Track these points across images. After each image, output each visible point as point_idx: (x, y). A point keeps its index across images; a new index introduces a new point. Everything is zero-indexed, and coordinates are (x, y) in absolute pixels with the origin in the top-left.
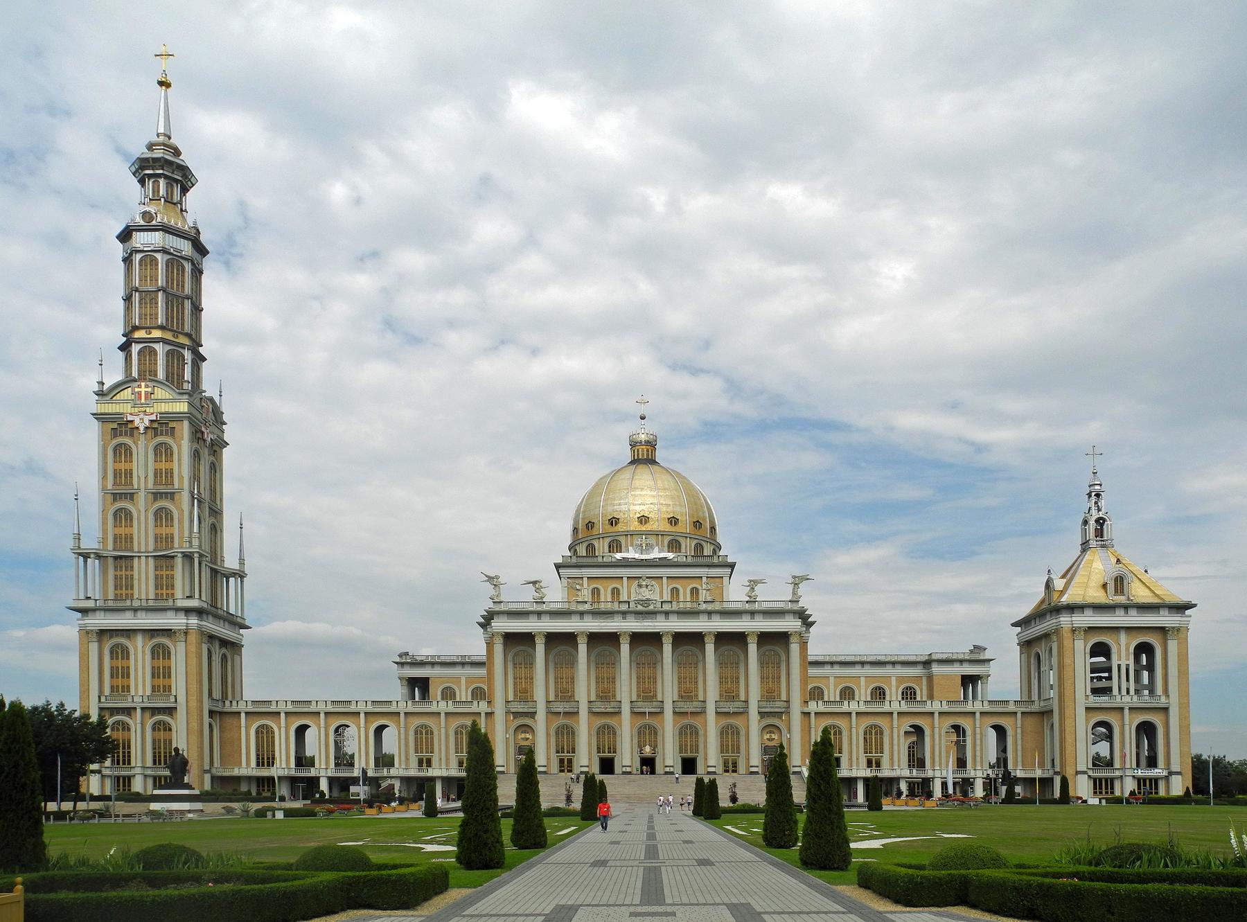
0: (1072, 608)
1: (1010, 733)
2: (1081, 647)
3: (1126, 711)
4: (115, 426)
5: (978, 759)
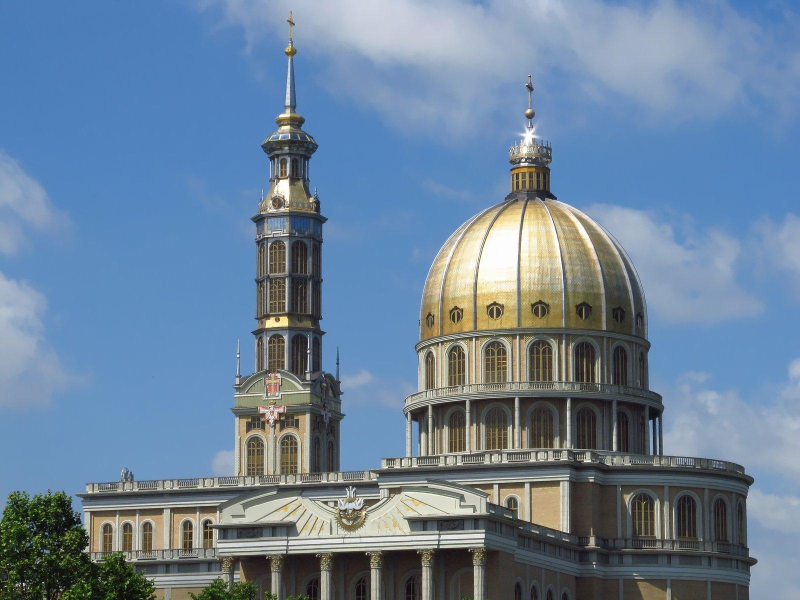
4: (250, 420)
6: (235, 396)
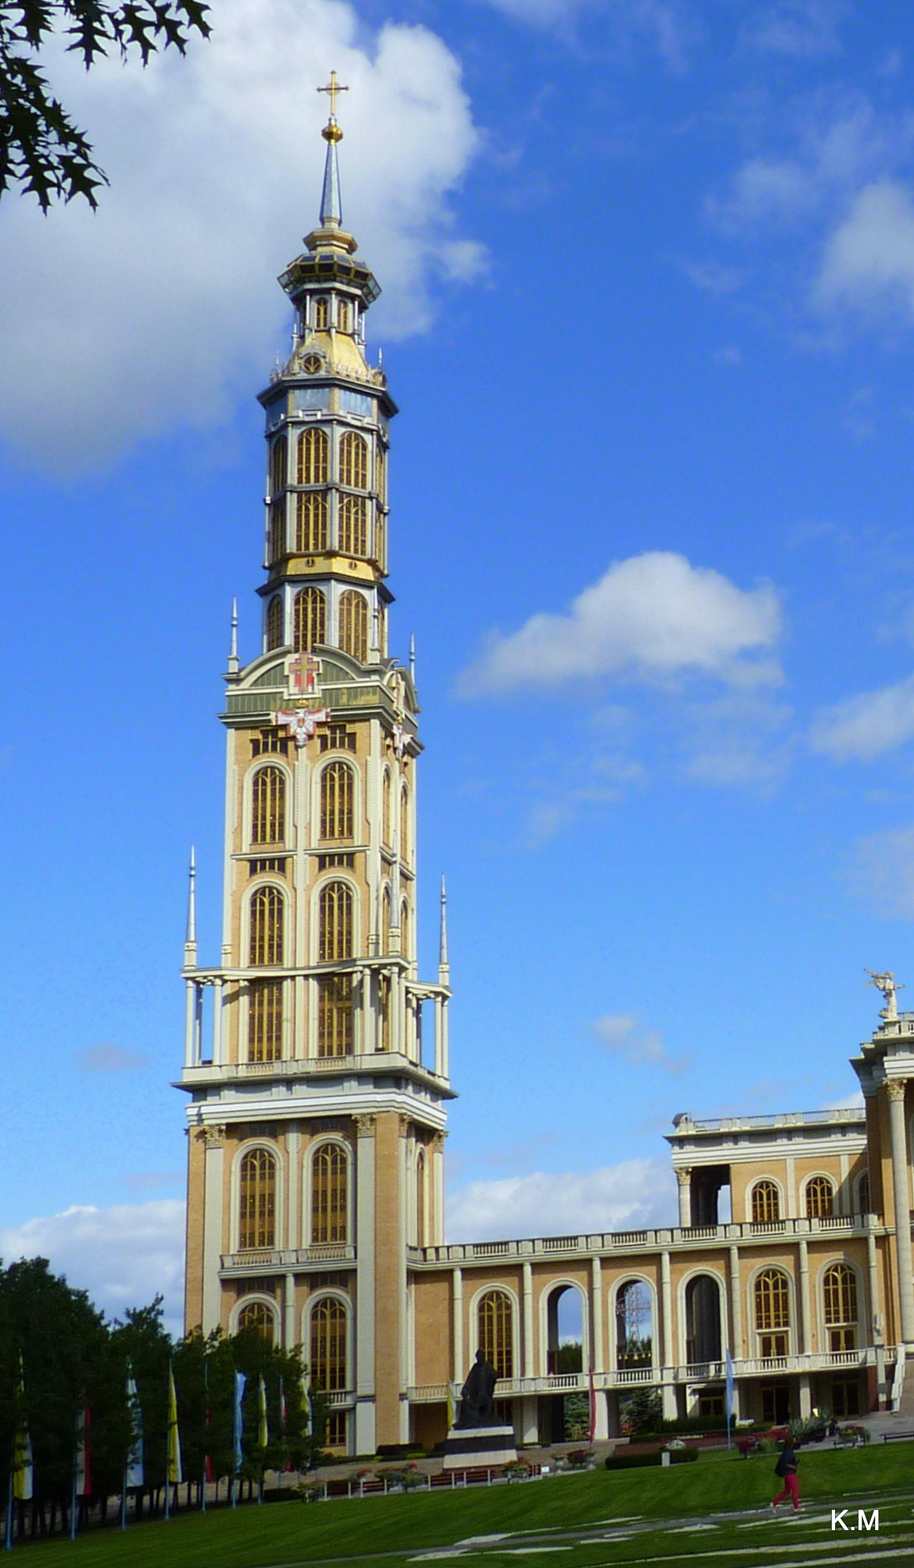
6: (228, 693)
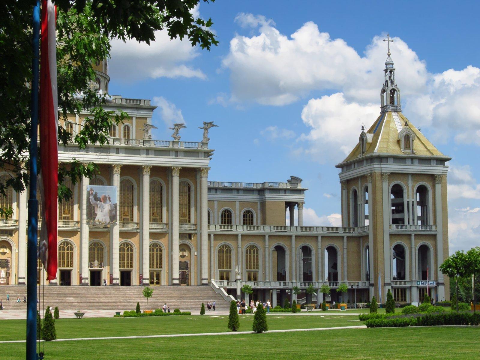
0: (382, 159)
1: (339, 253)
2: (386, 188)
3: (413, 237)
5: (320, 274)
